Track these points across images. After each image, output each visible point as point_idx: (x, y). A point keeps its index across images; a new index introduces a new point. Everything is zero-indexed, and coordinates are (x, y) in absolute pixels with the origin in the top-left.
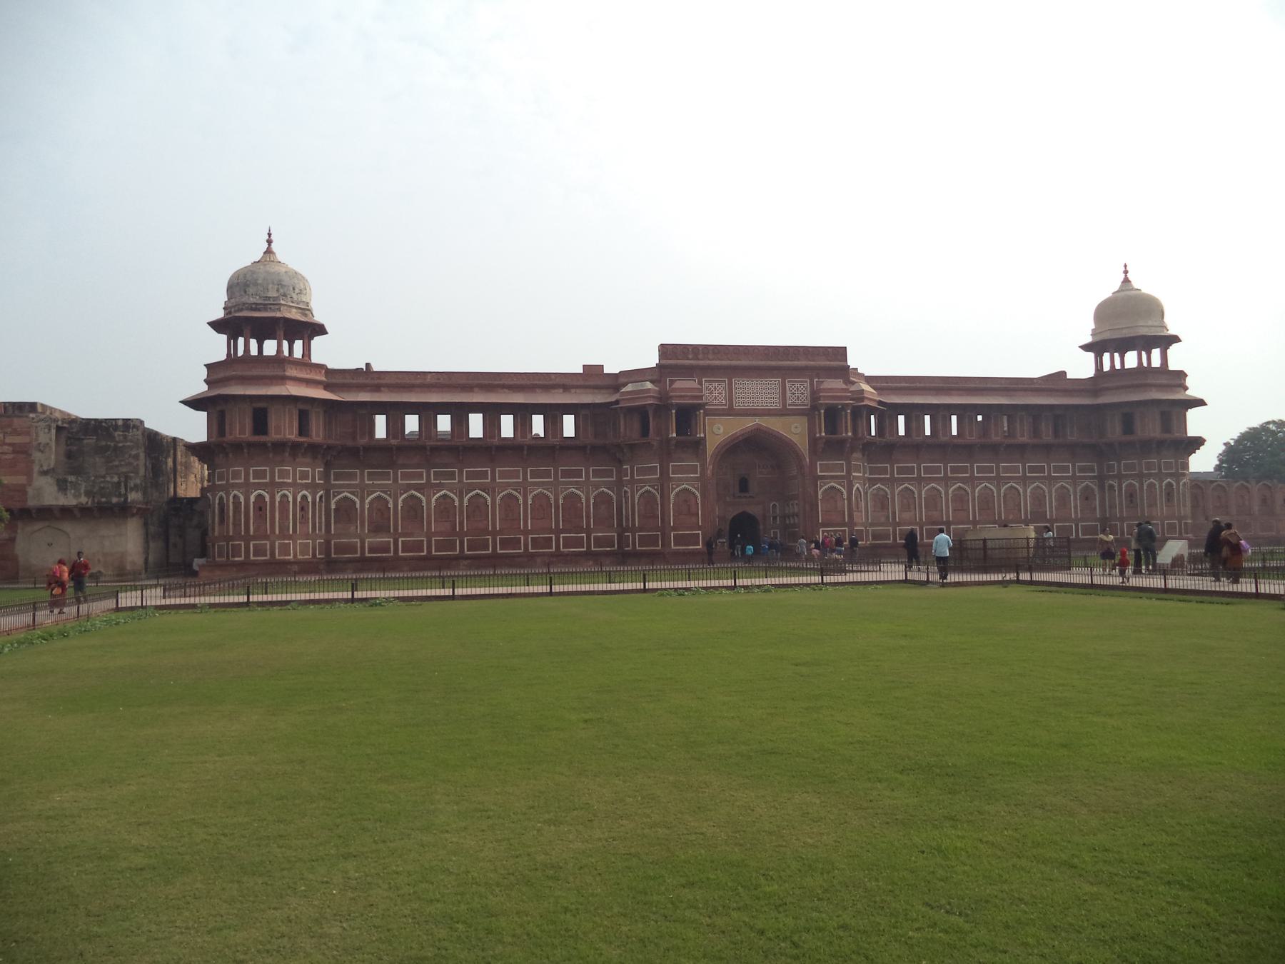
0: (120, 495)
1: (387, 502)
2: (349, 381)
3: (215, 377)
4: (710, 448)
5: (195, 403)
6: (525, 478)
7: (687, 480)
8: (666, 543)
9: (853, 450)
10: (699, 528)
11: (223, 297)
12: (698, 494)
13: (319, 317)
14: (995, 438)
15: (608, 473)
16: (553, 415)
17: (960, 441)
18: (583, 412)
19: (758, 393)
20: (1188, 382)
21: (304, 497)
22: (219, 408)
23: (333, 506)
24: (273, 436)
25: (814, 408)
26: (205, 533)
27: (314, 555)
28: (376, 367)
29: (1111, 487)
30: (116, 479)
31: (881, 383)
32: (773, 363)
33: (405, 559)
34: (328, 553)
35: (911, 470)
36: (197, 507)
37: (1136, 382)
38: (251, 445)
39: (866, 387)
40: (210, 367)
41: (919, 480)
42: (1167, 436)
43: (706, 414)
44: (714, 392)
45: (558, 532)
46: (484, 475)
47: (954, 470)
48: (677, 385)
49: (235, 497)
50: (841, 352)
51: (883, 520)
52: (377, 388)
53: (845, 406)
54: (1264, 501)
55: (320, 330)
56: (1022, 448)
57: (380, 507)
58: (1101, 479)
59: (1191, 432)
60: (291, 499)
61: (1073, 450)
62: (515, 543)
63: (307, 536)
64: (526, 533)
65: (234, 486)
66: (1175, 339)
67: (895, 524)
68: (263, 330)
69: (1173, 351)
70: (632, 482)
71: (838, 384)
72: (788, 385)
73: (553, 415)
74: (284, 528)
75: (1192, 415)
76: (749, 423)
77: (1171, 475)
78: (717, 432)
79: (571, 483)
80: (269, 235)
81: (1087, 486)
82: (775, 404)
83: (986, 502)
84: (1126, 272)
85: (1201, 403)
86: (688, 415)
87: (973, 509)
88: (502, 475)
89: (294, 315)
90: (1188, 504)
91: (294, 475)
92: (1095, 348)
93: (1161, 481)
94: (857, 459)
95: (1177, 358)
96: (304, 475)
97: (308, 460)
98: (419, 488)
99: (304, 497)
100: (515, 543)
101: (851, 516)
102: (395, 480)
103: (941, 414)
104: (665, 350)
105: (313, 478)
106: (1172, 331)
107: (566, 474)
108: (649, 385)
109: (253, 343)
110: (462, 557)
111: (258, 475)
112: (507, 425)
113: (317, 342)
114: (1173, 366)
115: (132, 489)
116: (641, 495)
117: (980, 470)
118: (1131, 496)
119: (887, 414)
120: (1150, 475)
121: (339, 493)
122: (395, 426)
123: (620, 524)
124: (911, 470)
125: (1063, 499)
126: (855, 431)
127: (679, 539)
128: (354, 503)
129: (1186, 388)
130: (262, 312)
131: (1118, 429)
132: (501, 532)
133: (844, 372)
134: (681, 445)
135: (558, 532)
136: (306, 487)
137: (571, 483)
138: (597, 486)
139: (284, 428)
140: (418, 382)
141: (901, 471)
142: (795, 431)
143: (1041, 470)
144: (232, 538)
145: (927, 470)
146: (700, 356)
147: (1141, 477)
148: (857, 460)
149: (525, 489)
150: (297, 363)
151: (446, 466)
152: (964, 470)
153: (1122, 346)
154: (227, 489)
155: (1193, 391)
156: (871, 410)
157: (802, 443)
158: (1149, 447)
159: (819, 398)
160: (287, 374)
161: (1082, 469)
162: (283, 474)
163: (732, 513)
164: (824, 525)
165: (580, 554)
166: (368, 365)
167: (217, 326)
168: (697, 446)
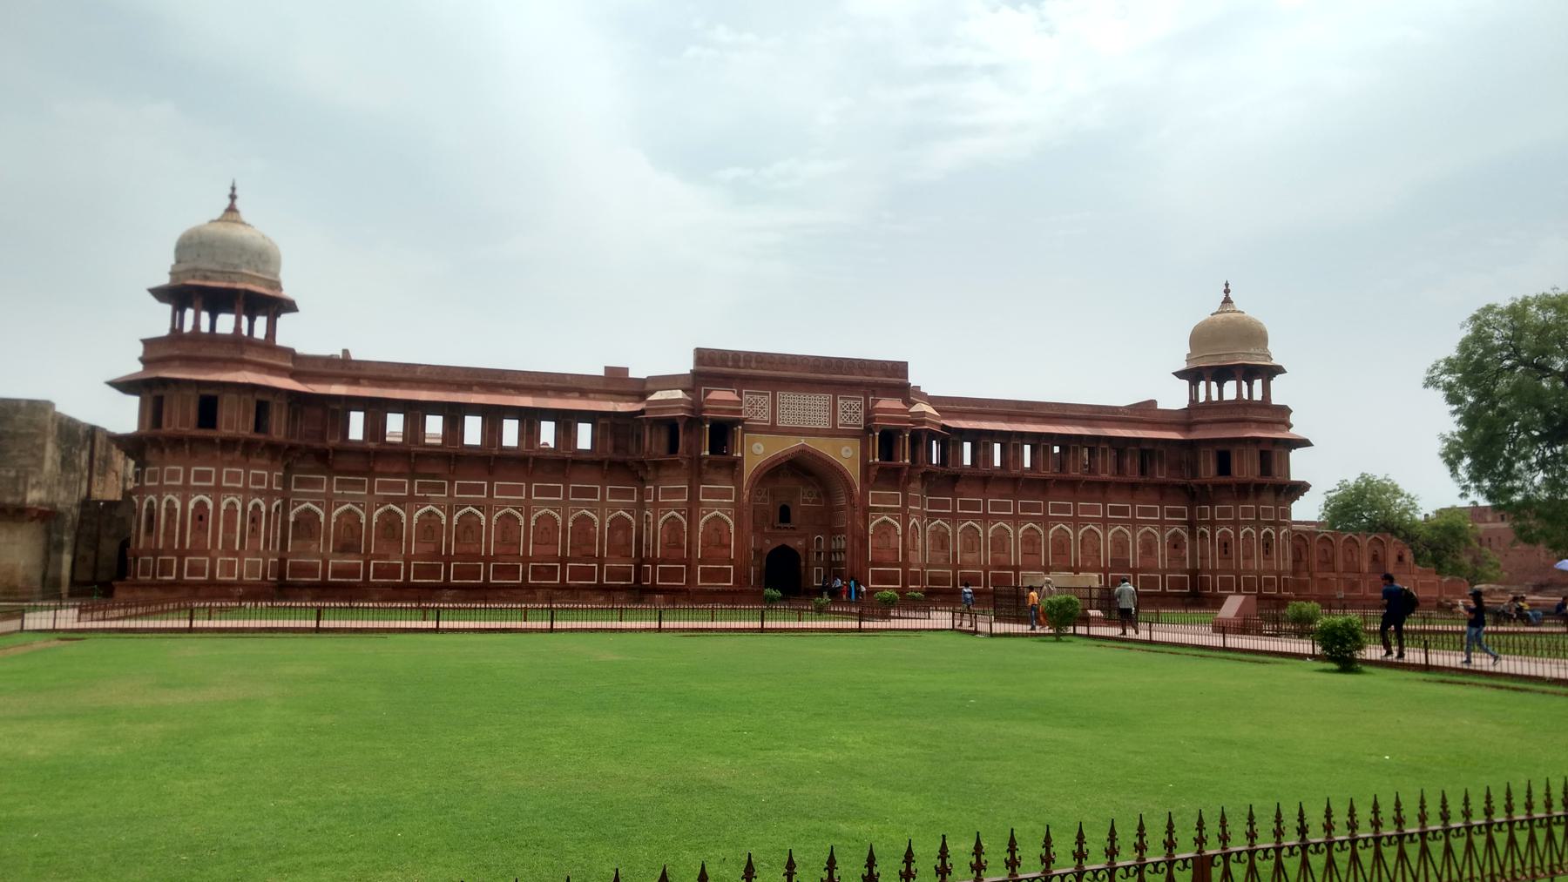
0: (16, 493)
5: (126, 386)
6: (529, 495)
7: (718, 505)
8: (691, 578)
9: (909, 479)
10: (731, 562)
11: (169, 260)
12: (732, 523)
13: (287, 292)
14: (1073, 474)
15: (629, 494)
16: (566, 422)
17: (1034, 475)
19: (807, 410)
20: (1292, 419)
21: (256, 507)
23: (292, 519)
24: (224, 430)
25: (869, 429)
26: (125, 545)
27: (264, 577)
28: (356, 355)
29: (1203, 534)
30: (12, 474)
31: (947, 405)
32: (823, 376)
33: (375, 585)
34: (281, 575)
35: (976, 506)
36: (119, 514)
37: (1233, 416)
39: (930, 409)
40: (149, 343)
41: (985, 518)
42: (1268, 480)
43: (744, 431)
44: (755, 407)
46: (479, 489)
47: (1025, 507)
48: (711, 396)
49: (170, 502)
50: (900, 368)
52: (355, 380)
53: (900, 431)
55: (290, 307)
56: (1104, 485)
58: (1191, 525)
59: (1295, 476)
60: (239, 507)
61: (1162, 490)
63: (257, 553)
64: (526, 559)
66: (1279, 370)
68: (217, 301)
70: (656, 504)
71: (897, 404)
73: (566, 422)
74: (228, 543)
75: (1295, 455)
76: (794, 443)
77: (1270, 523)
78: (757, 452)
79: (582, 503)
80: (233, 189)
81: (1176, 534)
82: (824, 423)
83: (1061, 546)
84: (1227, 292)
85: (1305, 443)
86: (724, 432)
88: (502, 491)
90: (1289, 557)
92: (1192, 375)
93: (1259, 530)
94: (915, 490)
95: (1281, 391)
96: (259, 480)
97: (264, 462)
98: (398, 501)
99: (256, 507)
102: (371, 491)
103: (1011, 441)
104: (702, 356)
105: (270, 483)
106: (1275, 362)
107: (577, 493)
108: (679, 394)
109: (205, 317)
110: (447, 586)
111: (201, 476)
112: (510, 433)
113: (284, 321)
114: (1276, 400)
115: (33, 487)
118: (1225, 546)
119: (951, 440)
120: (1246, 523)
121: (300, 503)
122: (375, 427)
123: (639, 551)
124: (976, 506)
125: (1148, 547)
126: (913, 459)
127: (707, 575)
128: (318, 516)
129: (1289, 426)
130: (220, 285)
131: (1213, 468)
133: (904, 391)
134: (715, 465)
135: (563, 560)
136: (259, 493)
138: (614, 508)
139: (234, 421)
141: (964, 505)
143: (1124, 511)
144: (162, 552)
145: (995, 506)
147: (1236, 524)
148: (915, 490)
151: (434, 476)
152: (1036, 508)
153: (1221, 374)
154: (159, 491)
155: (1296, 431)
156: (932, 435)
157: (854, 472)
158: (1244, 491)
159: (874, 419)
160: (246, 357)
161: (1170, 513)
162: (233, 477)
163: (769, 545)
164: (874, 564)
165: (589, 588)
166: (346, 352)
167: (160, 294)
168: (734, 466)
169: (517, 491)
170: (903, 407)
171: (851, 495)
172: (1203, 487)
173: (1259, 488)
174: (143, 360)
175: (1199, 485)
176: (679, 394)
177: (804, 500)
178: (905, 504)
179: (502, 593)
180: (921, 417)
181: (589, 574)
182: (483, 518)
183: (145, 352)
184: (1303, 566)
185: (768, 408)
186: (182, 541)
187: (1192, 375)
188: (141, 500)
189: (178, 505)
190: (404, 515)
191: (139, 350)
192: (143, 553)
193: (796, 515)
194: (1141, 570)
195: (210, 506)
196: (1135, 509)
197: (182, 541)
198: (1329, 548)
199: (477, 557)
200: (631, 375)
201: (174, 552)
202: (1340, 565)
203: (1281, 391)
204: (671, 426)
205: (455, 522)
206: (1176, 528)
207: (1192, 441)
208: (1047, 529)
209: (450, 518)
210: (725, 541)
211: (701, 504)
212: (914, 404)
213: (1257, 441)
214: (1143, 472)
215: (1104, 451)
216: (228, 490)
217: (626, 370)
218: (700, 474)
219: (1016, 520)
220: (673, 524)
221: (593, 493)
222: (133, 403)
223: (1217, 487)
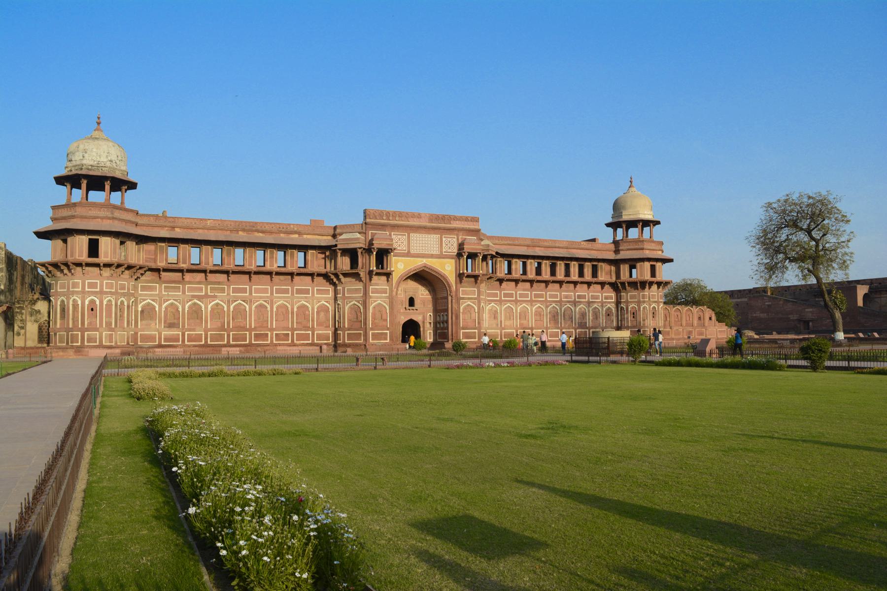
2: (152, 221)
3: (56, 216)
4: (395, 277)
6: (272, 293)
7: (380, 297)
8: (366, 339)
9: (482, 282)
10: (388, 329)
12: (388, 308)
13: (131, 178)
15: (327, 292)
18: (310, 251)
20: (664, 247)
21: (122, 302)
23: (140, 309)
24: (103, 258)
25: (459, 255)
27: (128, 343)
29: (622, 308)
33: (189, 346)
34: (135, 340)
35: (511, 295)
38: (88, 265)
40: (54, 208)
41: (516, 301)
45: (293, 330)
47: (536, 296)
49: (74, 300)
54: (700, 318)
55: (132, 186)
60: (113, 303)
63: (124, 329)
64: (272, 330)
65: (73, 293)
74: (109, 324)
79: (302, 298)
80: (99, 118)
82: (436, 251)
85: (671, 260)
86: (383, 255)
88: (257, 291)
89: (118, 175)
92: (614, 225)
93: (650, 305)
98: (199, 298)
102: (184, 292)
105: (129, 289)
107: (299, 291)
108: (358, 235)
111: (91, 285)
116: (350, 308)
117: (551, 296)
120: (644, 302)
121: (144, 300)
127: (375, 336)
128: (154, 307)
131: (627, 274)
134: (378, 274)
135: (293, 330)
136: (124, 295)
137: (302, 298)
141: (506, 295)
142: (447, 269)
144: (72, 330)
147: (639, 303)
149: (272, 301)
150: (115, 207)
151: (219, 283)
152: (541, 296)
154: (68, 294)
155: (666, 255)
157: (452, 278)
163: (403, 319)
164: (463, 329)
167: (60, 180)
169: (265, 291)
172: (623, 284)
173: (651, 284)
174: (53, 219)
178: (479, 295)
179: (259, 349)
181: (306, 337)
182: (247, 307)
183: (54, 214)
184: (667, 322)
185: (405, 243)
186: (83, 323)
187: (614, 225)
188: (56, 301)
189: (80, 302)
190: (203, 306)
191: (50, 213)
192: (60, 330)
193: (417, 302)
194: (592, 328)
195: (98, 303)
197: (83, 323)
198: (679, 314)
199: (244, 328)
200: (326, 224)
202: (684, 323)
204: (352, 254)
205: (232, 309)
206: (609, 305)
208: (547, 307)
209: (229, 307)
210: (384, 317)
211: (370, 297)
212: (482, 240)
216: (106, 293)
217: (323, 221)
218: (370, 280)
219: (531, 302)
220: (355, 309)
221: (307, 292)
223: (629, 283)
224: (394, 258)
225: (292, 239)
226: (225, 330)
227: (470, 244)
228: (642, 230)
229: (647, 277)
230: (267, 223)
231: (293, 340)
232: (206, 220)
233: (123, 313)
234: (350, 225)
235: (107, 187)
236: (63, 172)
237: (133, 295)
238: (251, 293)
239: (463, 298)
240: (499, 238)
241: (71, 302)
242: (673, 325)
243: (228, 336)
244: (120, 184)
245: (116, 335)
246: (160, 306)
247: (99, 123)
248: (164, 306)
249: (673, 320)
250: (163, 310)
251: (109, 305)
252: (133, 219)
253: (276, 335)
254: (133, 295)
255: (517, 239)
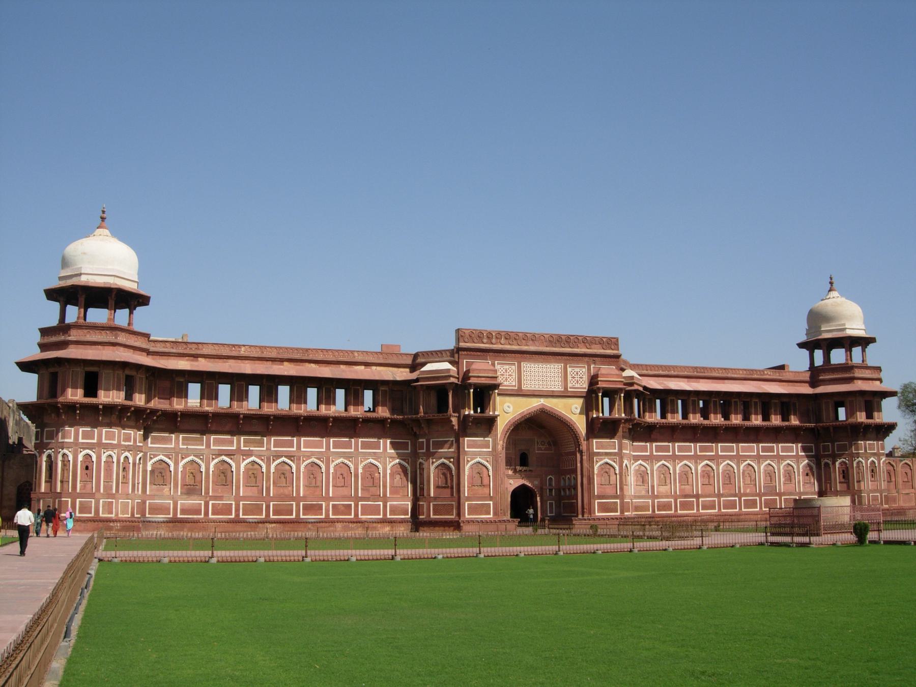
1: (200, 466)
4: (502, 425)
5: (25, 366)
6: (328, 448)
7: (480, 454)
10: (491, 498)
12: (490, 468)
15: (405, 446)
19: (543, 376)
20: (882, 375)
22: (52, 370)
23: (149, 468)
29: (827, 465)
33: (214, 521)
38: (84, 406)
41: (674, 458)
43: (499, 394)
44: (505, 373)
45: (357, 499)
48: (474, 367)
51: (643, 493)
52: (195, 356)
57: (194, 470)
60: (115, 460)
62: (317, 509)
63: (127, 496)
64: (328, 499)
67: (654, 497)
69: (871, 347)
72: (569, 370)
74: (108, 488)
76: (534, 404)
77: (874, 454)
78: (507, 411)
82: (558, 387)
84: (831, 283)
86: (484, 394)
87: (719, 484)
91: (119, 436)
92: (810, 346)
95: (873, 356)
98: (229, 454)
100: (317, 509)
101: (622, 489)
102: (208, 446)
108: (446, 366)
113: (139, 310)
114: (870, 362)
121: (155, 456)
125: (789, 477)
131: (832, 415)
132: (304, 498)
133: (615, 358)
135: (357, 499)
140: (234, 354)
146: (494, 341)
156: (638, 394)
157: (580, 424)
162: (110, 436)
164: (599, 497)
168: (490, 422)
170: (617, 372)
171: (578, 445)
172: (827, 429)
174: (43, 347)
175: (823, 428)
176: (446, 366)
177: (538, 450)
178: (620, 449)
180: (630, 382)
185: (515, 375)
187: (810, 346)
191: (37, 337)
193: (532, 459)
194: (784, 494)
196: (779, 448)
198: (908, 471)
200: (402, 351)
201: (69, 495)
203: (873, 356)
204: (440, 392)
205: (272, 470)
207: (816, 395)
208: (718, 465)
210: (485, 482)
211: (466, 453)
212: (623, 370)
213: (862, 393)
214: (783, 420)
215: (756, 403)
219: (696, 458)
222: (32, 379)
224: (498, 399)
225: (356, 372)
226: (261, 498)
227: (604, 375)
228: (851, 351)
229: (861, 417)
230: (322, 350)
231: (356, 514)
232: (239, 346)
233: (128, 474)
234: (436, 352)
235: (111, 303)
236: (55, 284)
237: (140, 449)
238: (299, 447)
239: (598, 454)
240: (647, 367)
241: (60, 458)
242: (900, 486)
243: (268, 507)
244: (129, 300)
245: (117, 503)
246: (176, 464)
247: (103, 219)
248: (181, 464)
249: (900, 480)
250: (180, 469)
251: (109, 462)
252: (144, 346)
253: (334, 506)
254: (140, 449)
255: (674, 368)
